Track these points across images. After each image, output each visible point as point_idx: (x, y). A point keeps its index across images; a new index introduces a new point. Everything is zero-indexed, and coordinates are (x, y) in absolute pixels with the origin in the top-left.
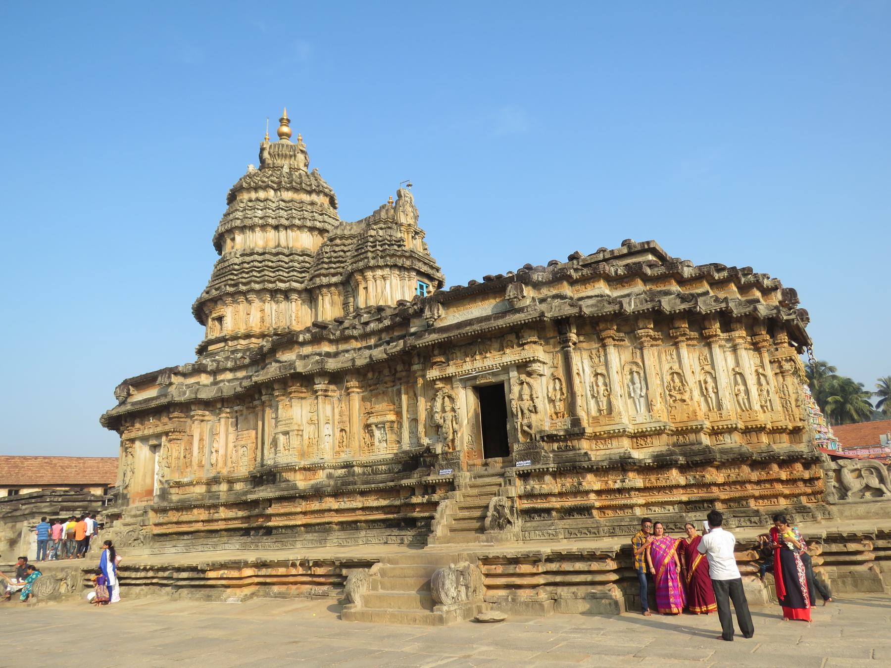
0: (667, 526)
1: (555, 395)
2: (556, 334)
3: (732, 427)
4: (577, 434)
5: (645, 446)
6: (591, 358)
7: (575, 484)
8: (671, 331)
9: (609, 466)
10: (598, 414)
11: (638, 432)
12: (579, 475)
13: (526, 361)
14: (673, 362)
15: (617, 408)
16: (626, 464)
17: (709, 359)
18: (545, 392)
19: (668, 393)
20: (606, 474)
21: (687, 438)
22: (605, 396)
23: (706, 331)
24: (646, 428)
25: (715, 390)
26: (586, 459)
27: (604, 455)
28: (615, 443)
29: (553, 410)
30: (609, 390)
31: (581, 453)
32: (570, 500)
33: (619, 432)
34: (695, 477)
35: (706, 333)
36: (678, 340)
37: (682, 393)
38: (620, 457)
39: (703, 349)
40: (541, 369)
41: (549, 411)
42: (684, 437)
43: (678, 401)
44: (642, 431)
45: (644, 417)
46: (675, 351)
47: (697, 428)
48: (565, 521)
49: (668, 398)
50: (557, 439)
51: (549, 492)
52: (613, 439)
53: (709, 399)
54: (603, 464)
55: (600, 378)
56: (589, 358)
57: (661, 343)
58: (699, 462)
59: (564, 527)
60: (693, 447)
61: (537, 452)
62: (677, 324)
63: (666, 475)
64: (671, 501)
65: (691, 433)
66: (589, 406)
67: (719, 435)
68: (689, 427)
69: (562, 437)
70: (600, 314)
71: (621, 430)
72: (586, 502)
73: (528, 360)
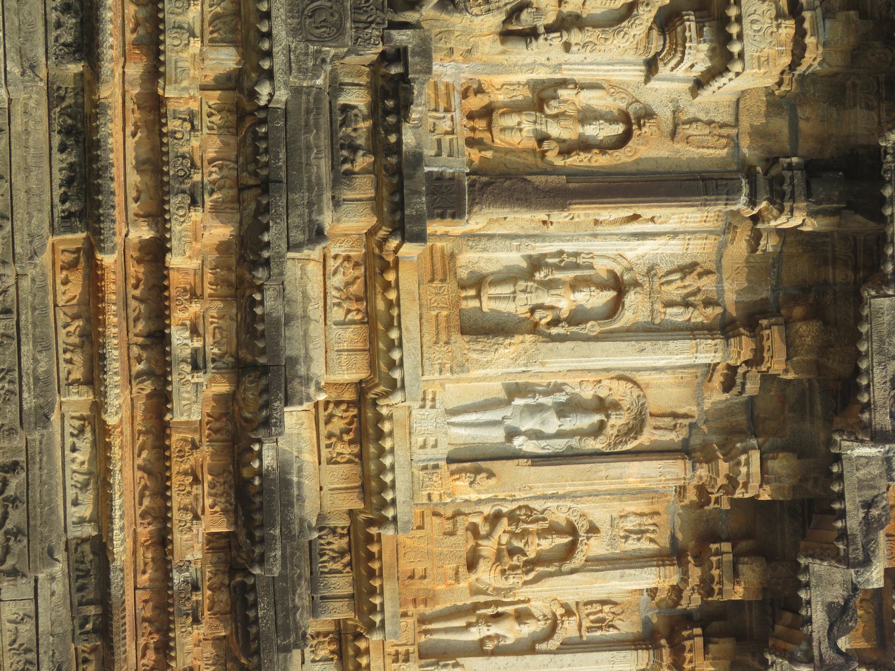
0: (14, 500)
1: (563, 114)
2: (806, 146)
4: (399, 207)
5: (324, 431)
6: (686, 270)
7: (197, 177)
8: (726, 547)
9: (262, 319)
10: (463, 274)
11: (380, 418)
12: (233, 192)
13: (727, 21)
14: (613, 538)
15: (484, 358)
16: (266, 390)
18: (579, 75)
19: (505, 510)
20: (225, 290)
21: (338, 566)
22: (532, 311)
23: (699, 641)
24: (392, 451)
25: (490, 646)
26: (298, 236)
27: (305, 294)
28: (350, 337)
29: (501, 97)
30: (554, 331)
31: (320, 212)
32: (131, 142)
33: (392, 365)
34: (196, 588)
35: (691, 637)
36: (691, 566)
37: (498, 558)
38: (293, 361)
39: (636, 618)
40: (680, 72)
41: (498, 80)
42: (342, 554)
43: (471, 543)
44: (380, 435)
45: (431, 441)
46: (656, 547)
47: (373, 609)
48: (43, 112)
49: (488, 510)
50: (387, 112)
51: (169, 69)
52: (364, 330)
53: (461, 623)
54: (269, 293)
55: (598, 299)
56: (688, 261)
57: (686, 502)
58: (251, 614)
59: (18, 109)
60: (303, 589)
61: (340, 29)
62: (751, 572)
63: (208, 501)
64: (110, 519)
65: (356, 583)
66: (501, 243)
67: (333, 647)
68: (377, 583)
69: (393, 138)
70: (863, 348)
71: (397, 375)
72: (117, 214)
73: (734, 30)
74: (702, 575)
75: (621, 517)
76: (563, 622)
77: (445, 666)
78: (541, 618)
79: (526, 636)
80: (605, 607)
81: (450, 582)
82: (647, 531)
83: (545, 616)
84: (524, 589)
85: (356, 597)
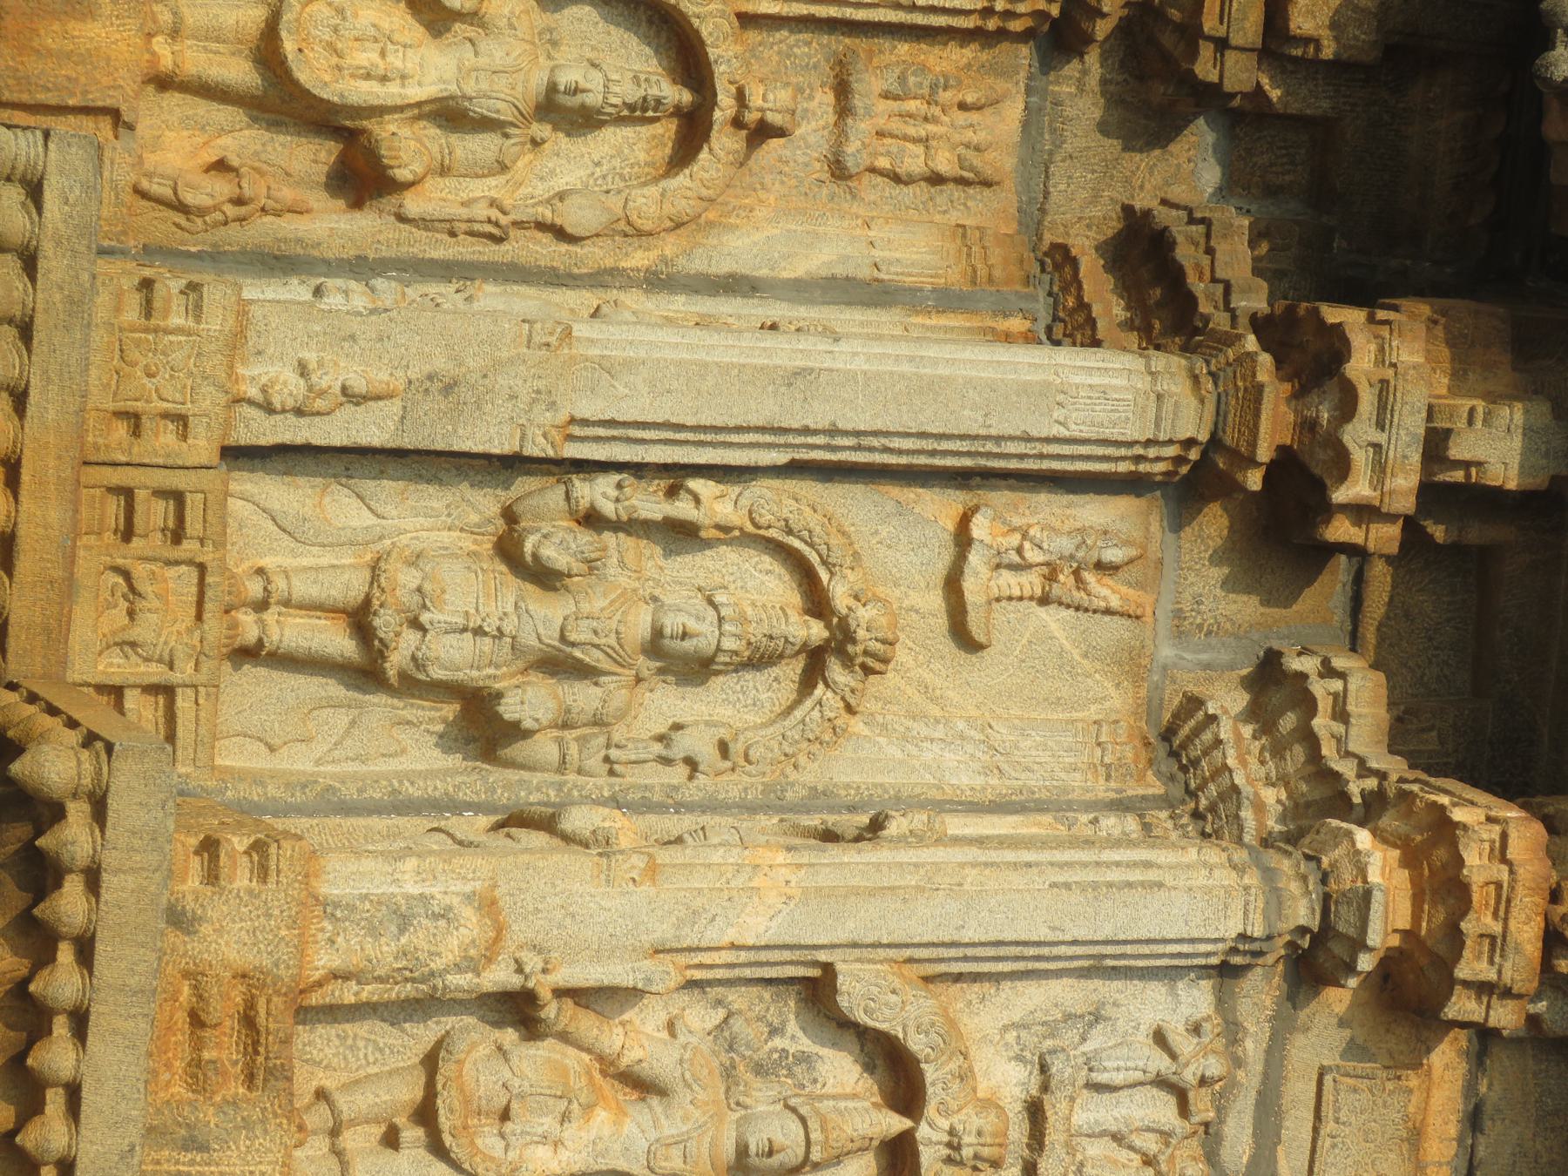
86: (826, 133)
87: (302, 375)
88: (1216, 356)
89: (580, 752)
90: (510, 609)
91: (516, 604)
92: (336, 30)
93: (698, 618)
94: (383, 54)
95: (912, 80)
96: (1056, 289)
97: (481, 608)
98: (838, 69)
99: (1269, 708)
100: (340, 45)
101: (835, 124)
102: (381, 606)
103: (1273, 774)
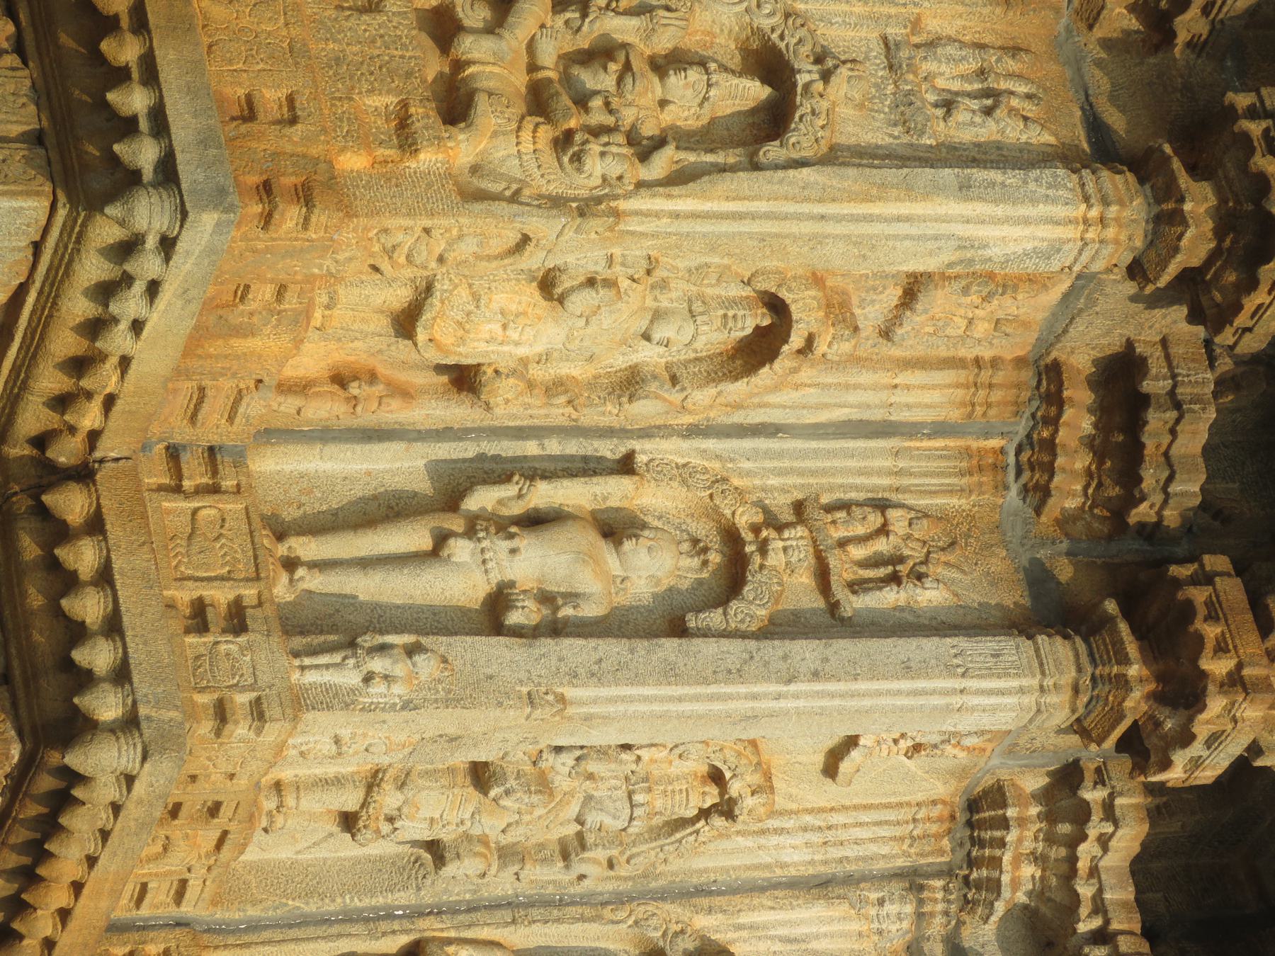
3: (84, 679)
14: (905, 103)
17: (889, 598)
23: (1232, 590)
39: (998, 563)
43: (434, 66)
46: (1051, 140)
53: (414, 537)
68: (126, 51)
74: (1223, 200)
75: (917, 46)
76: (763, 548)
77: (383, 648)
78: (686, 546)
79: (647, 600)
80: (892, 514)
81: (382, 152)
82: (1012, 93)
83: (695, 541)
84: (642, 203)
85: (50, 140)
86: (885, 311)
87: (336, 743)
88: (1104, 665)
89: (498, 871)
90: (467, 816)
91: (473, 814)
92: (468, 315)
93: (614, 817)
94: (505, 327)
95: (975, 288)
96: (1039, 414)
97: (444, 817)
98: (912, 280)
99: (1058, 805)
100: (467, 327)
101: (896, 306)
102: (365, 827)
103: (1040, 850)
